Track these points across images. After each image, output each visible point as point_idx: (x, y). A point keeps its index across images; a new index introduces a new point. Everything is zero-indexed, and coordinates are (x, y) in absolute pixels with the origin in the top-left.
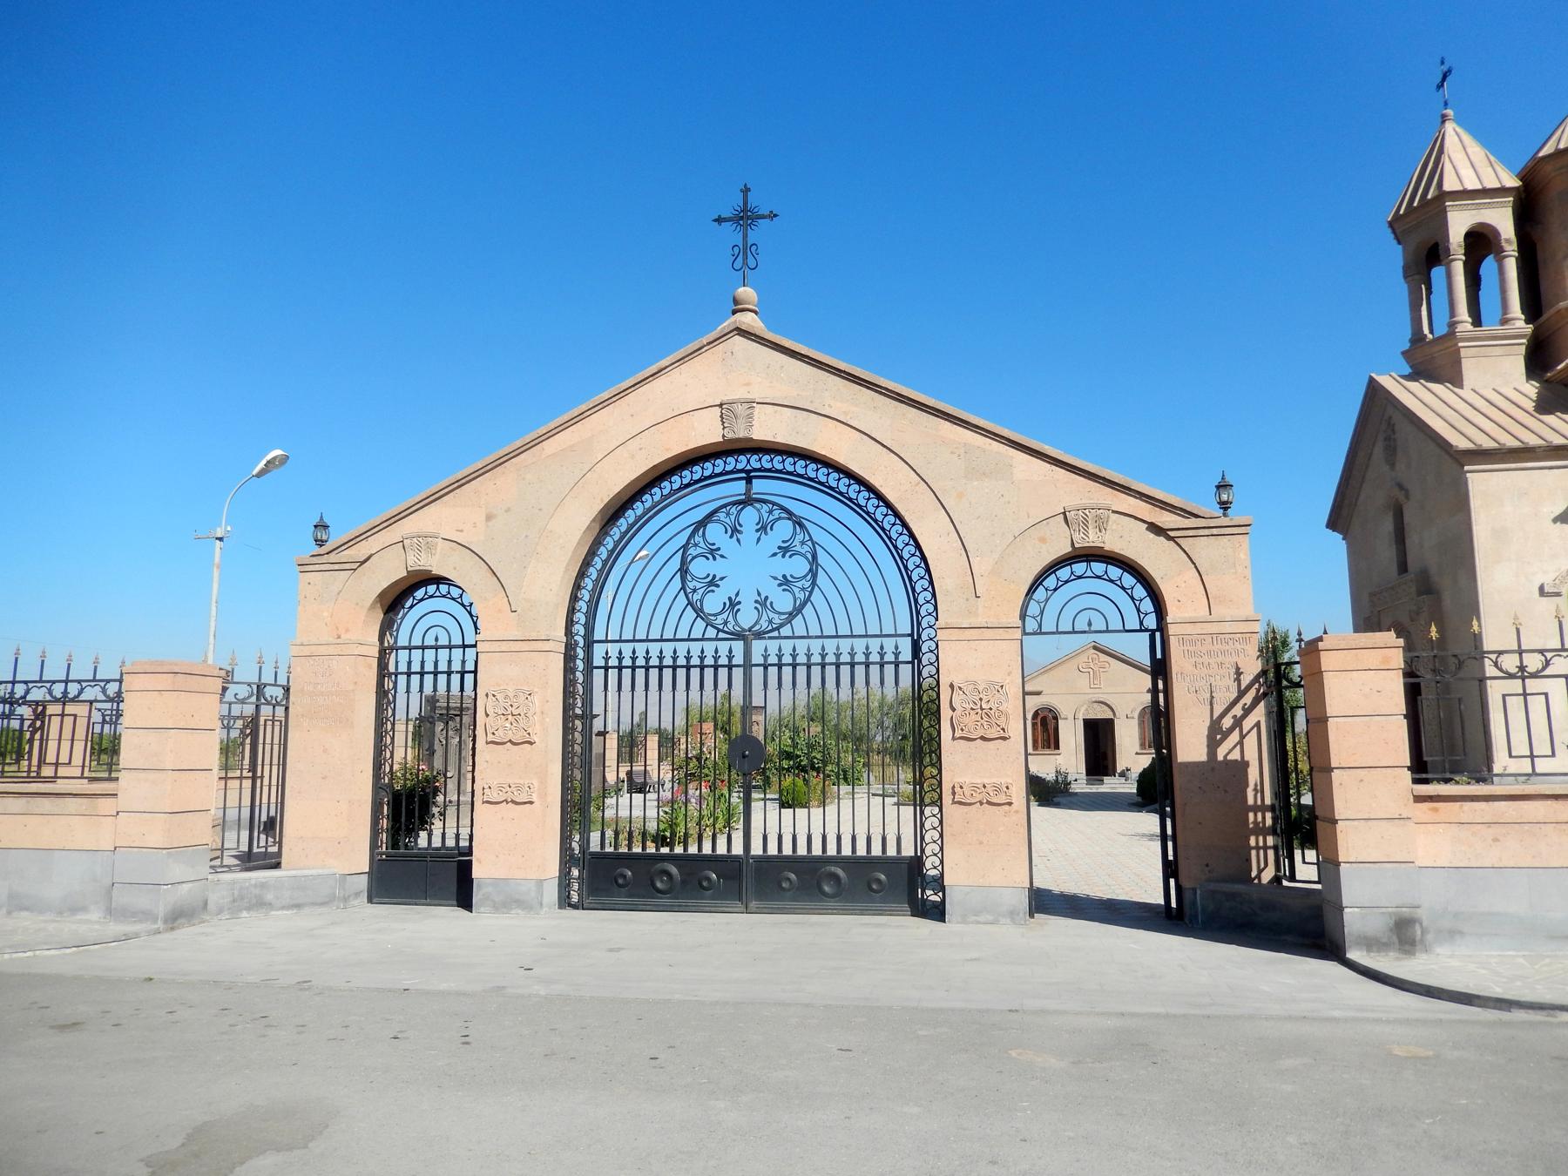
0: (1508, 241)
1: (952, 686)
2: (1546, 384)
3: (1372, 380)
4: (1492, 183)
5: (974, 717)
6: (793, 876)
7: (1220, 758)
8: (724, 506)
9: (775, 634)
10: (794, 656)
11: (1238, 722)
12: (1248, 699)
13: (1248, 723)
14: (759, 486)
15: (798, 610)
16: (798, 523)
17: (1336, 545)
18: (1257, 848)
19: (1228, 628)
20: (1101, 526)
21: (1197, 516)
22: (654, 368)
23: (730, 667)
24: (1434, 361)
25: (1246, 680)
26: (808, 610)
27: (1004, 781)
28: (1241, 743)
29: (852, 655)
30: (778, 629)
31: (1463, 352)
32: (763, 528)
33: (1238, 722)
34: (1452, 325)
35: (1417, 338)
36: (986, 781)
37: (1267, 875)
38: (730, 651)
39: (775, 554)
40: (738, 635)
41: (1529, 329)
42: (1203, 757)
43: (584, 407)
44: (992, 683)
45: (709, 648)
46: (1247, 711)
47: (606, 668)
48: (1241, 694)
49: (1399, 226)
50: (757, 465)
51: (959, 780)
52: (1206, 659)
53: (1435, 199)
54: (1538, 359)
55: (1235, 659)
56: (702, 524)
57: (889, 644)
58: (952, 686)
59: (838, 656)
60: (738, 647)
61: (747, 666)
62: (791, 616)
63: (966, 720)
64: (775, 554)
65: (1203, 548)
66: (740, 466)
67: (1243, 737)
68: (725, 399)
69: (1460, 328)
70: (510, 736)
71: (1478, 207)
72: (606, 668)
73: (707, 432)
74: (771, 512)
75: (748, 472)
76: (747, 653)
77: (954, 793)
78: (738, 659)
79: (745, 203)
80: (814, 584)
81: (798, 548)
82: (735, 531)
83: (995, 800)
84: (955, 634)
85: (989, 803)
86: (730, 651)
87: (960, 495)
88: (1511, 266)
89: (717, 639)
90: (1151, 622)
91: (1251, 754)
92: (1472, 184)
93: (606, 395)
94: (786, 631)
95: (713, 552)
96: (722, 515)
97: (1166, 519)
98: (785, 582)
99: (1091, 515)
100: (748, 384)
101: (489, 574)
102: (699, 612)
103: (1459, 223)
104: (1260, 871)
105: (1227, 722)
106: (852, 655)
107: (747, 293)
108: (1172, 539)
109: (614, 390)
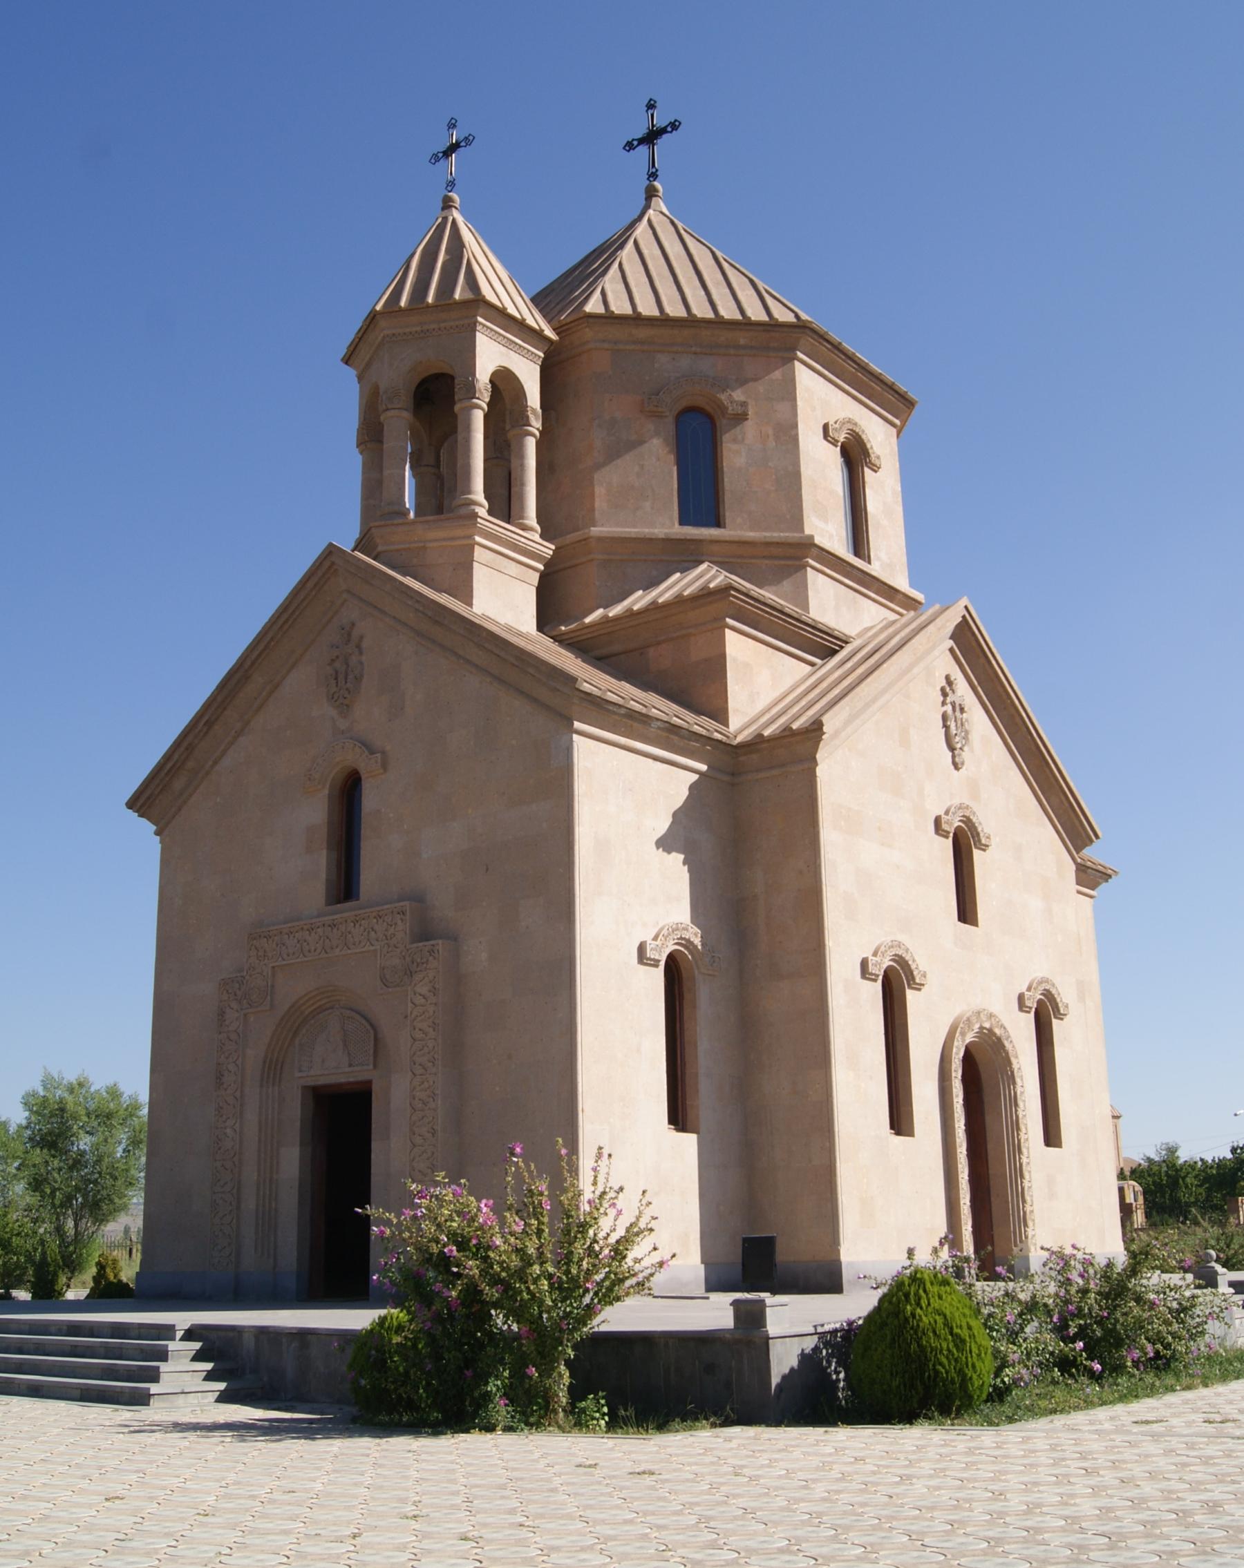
0: (534, 410)
17: (142, 841)
31: (479, 553)
41: (548, 549)
53: (464, 303)
71: (509, 345)
103: (491, 354)
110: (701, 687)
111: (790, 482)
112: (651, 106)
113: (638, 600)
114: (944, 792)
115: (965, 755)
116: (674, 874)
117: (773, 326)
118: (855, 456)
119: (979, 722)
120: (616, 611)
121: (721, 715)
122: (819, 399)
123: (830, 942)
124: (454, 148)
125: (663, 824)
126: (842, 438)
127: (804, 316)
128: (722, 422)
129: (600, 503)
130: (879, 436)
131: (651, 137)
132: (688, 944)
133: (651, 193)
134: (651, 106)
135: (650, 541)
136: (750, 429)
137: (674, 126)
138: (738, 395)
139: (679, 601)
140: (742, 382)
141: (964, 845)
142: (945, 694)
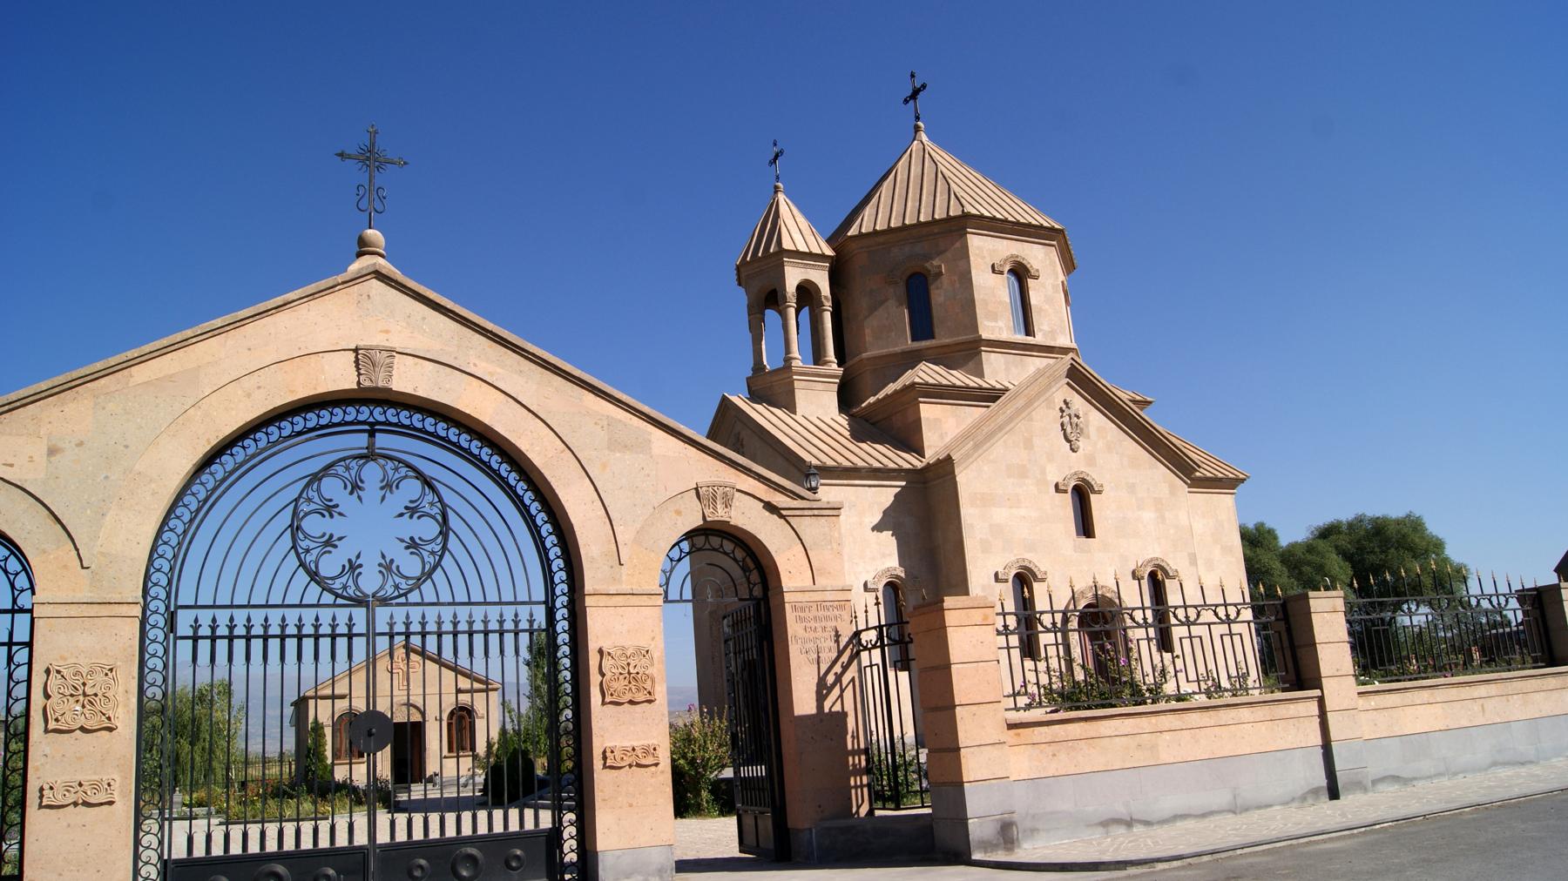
1: (601, 652)
2: (853, 419)
3: (724, 399)
4: (816, 250)
5: (623, 682)
6: (423, 862)
7: (826, 710)
8: (344, 459)
9: (402, 600)
10: (423, 624)
11: (839, 678)
12: (845, 658)
13: (846, 679)
14: (382, 440)
15: (428, 575)
16: (427, 483)
18: (856, 787)
19: (829, 596)
20: (727, 505)
21: (803, 498)
22: (279, 300)
23: (350, 636)
24: (773, 388)
25: (844, 641)
26: (438, 575)
27: (652, 742)
28: (841, 696)
29: (486, 622)
30: (405, 595)
32: (388, 486)
33: (839, 678)
34: (788, 360)
35: (758, 367)
36: (635, 744)
37: (864, 811)
38: (350, 619)
39: (401, 515)
40: (359, 602)
41: (840, 371)
42: (813, 711)
43: (189, 333)
44: (639, 649)
45: (326, 615)
46: (845, 668)
47: (195, 639)
48: (840, 653)
49: (744, 274)
50: (382, 419)
51: (609, 744)
52: (813, 624)
53: (775, 253)
54: (847, 398)
55: (833, 624)
56: (316, 478)
57: (524, 612)
58: (601, 652)
59: (471, 623)
60: (359, 614)
61: (371, 635)
62: (419, 582)
63: (615, 685)
64: (401, 515)
65: (806, 526)
66: (361, 418)
67: (842, 691)
68: (361, 344)
69: (794, 363)
70: (81, 721)
72: (195, 639)
73: (340, 376)
74: (396, 469)
75: (372, 424)
76: (371, 621)
77: (605, 758)
78: (360, 627)
79: (373, 145)
80: (444, 548)
81: (427, 509)
82: (356, 487)
83: (644, 762)
84: (603, 600)
85: (638, 765)
86: (350, 619)
87: (604, 466)
88: (827, 317)
89: (334, 605)
90: (757, 592)
91: (849, 707)
92: (803, 248)
93: (218, 322)
94: (414, 597)
95: (330, 509)
96: (340, 470)
97: (780, 500)
98: (413, 545)
99: (720, 491)
100: (387, 332)
101: (50, 521)
102: (314, 576)
103: (793, 276)
104: (859, 807)
105: (831, 679)
106: (486, 622)
107: (373, 234)
108: (782, 517)
109: (228, 318)
110: (909, 440)
111: (969, 305)
112: (913, 76)
113: (891, 388)
114: (1065, 467)
115: (1082, 443)
116: (888, 540)
117: (949, 219)
118: (1020, 273)
119: (1094, 419)
120: (881, 395)
121: (920, 452)
122: (984, 250)
123: (969, 567)
124: (777, 156)
125: (877, 518)
126: (1007, 268)
127: (969, 209)
128: (930, 279)
129: (868, 339)
130: (1040, 257)
131: (915, 94)
132: (898, 577)
133: (917, 129)
134: (913, 76)
135: (895, 355)
136: (945, 280)
137: (924, 86)
138: (936, 263)
139: (896, 392)
140: (939, 253)
141: (1082, 495)
142: (1062, 410)
